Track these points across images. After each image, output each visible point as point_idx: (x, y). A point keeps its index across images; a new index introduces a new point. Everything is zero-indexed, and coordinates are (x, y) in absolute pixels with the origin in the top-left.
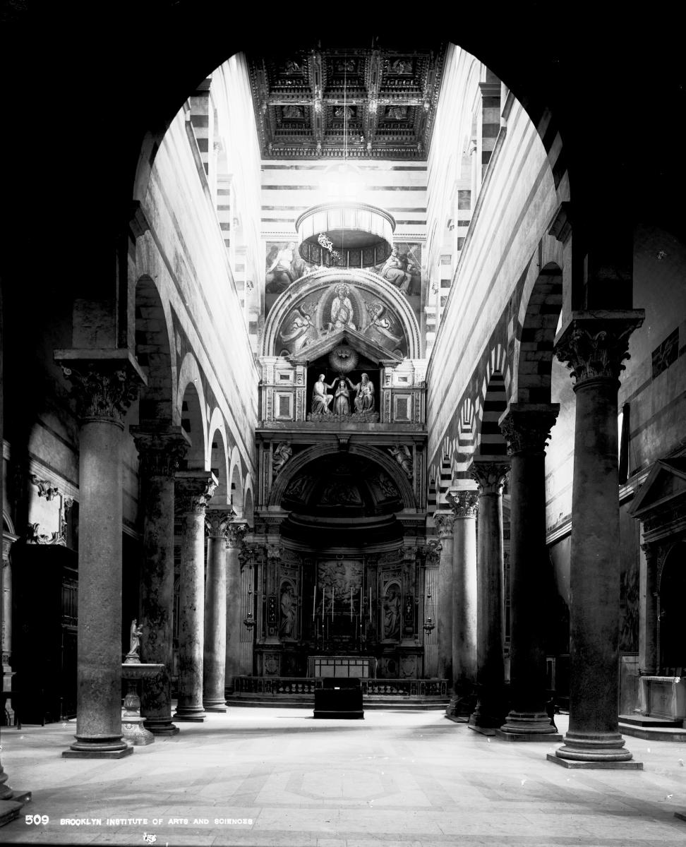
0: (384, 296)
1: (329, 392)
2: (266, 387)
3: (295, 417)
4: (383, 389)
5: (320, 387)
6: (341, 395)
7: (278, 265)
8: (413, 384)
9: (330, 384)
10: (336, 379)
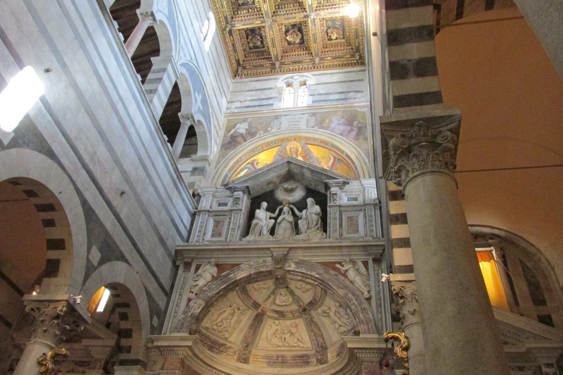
0: (333, 146)
2: (200, 211)
3: (226, 238)
4: (330, 207)
5: (262, 214)
6: (284, 219)
7: (235, 132)
9: (274, 212)
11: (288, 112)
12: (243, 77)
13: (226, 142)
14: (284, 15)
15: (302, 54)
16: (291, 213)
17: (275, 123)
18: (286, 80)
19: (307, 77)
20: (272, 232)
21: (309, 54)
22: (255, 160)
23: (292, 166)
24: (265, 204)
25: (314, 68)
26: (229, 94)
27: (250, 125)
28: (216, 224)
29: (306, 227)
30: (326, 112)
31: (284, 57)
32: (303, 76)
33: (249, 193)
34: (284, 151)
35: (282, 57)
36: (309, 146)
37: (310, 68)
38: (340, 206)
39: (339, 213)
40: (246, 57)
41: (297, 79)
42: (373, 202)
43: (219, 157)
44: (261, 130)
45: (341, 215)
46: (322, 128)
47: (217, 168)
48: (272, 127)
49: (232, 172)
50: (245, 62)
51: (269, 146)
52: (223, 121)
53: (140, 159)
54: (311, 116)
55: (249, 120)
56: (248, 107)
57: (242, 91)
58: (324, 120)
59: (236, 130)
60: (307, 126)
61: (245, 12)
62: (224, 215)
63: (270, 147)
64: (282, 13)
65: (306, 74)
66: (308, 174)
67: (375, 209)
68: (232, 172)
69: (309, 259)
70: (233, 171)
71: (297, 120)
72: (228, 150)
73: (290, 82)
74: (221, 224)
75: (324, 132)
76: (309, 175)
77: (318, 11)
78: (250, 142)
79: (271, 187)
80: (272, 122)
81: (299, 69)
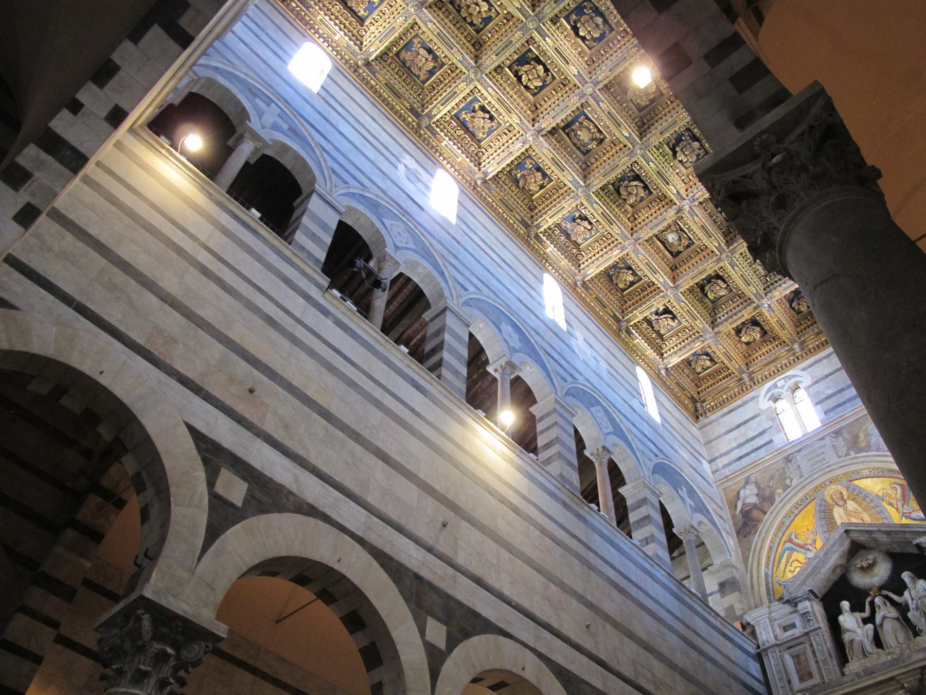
1: (865, 621)
2: (765, 650)
3: (822, 677)
5: (848, 620)
6: (884, 618)
7: (743, 505)
9: (863, 611)
10: (869, 599)
11: (801, 446)
12: (709, 414)
13: (740, 525)
14: (726, 320)
15: (772, 349)
16: (888, 604)
17: (791, 469)
18: (769, 394)
19: (795, 376)
20: (878, 641)
21: (780, 344)
22: (790, 534)
23: (854, 536)
24: (845, 605)
25: (798, 358)
26: (704, 448)
27: (757, 485)
30: (852, 422)
31: (750, 364)
32: (790, 377)
33: (816, 596)
34: (823, 503)
35: (747, 364)
36: (856, 482)
37: (792, 362)
40: (698, 387)
41: (784, 386)
43: (743, 553)
44: (777, 488)
46: (861, 450)
47: (749, 570)
48: (790, 478)
49: (771, 566)
50: (702, 394)
51: (800, 506)
52: (716, 492)
53: (684, 639)
54: (836, 438)
55: (753, 479)
56: (740, 458)
57: (719, 437)
58: (857, 437)
59: (744, 501)
60: (839, 457)
61: (674, 339)
62: (801, 644)
63: (802, 507)
64: (723, 318)
65: (791, 373)
66: (883, 538)
68: (771, 566)
70: (771, 563)
71: (819, 452)
72: (749, 537)
73: (776, 394)
74: (802, 658)
75: (867, 456)
76: (886, 539)
77: (770, 295)
78: (772, 513)
79: (839, 572)
80: (786, 470)
81: (778, 370)
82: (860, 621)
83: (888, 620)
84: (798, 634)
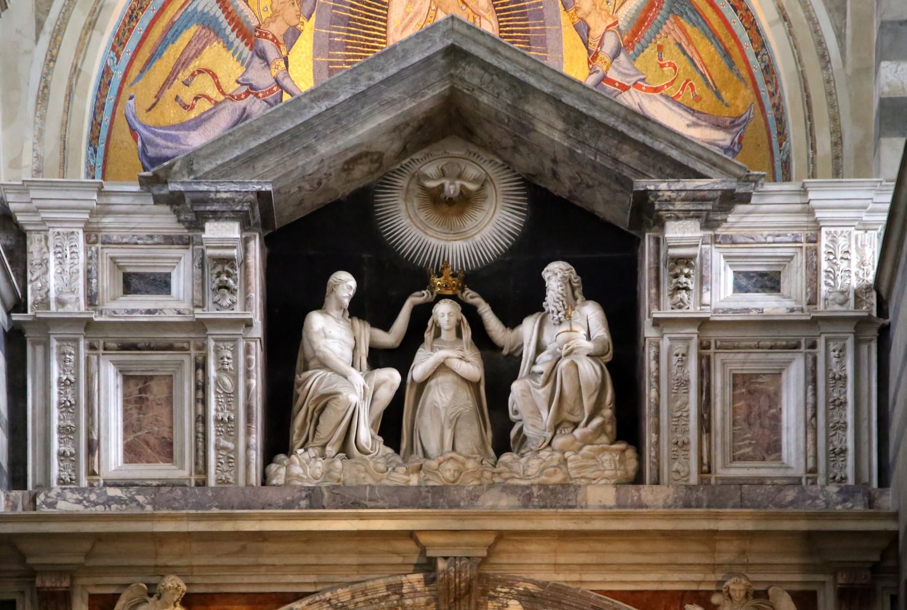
2: (45, 325)
4: (657, 323)
6: (442, 367)
8: (812, 302)
9: (385, 325)
10: (415, 299)
16: (467, 333)
28: (134, 390)
29: (547, 417)
38: (703, 323)
39: (700, 357)
42: (849, 309)
45: (705, 370)
62: (170, 347)
67: (857, 343)
69: (575, 577)
74: (157, 390)
82: (364, 351)
83: (450, 377)
84: (170, 317)
